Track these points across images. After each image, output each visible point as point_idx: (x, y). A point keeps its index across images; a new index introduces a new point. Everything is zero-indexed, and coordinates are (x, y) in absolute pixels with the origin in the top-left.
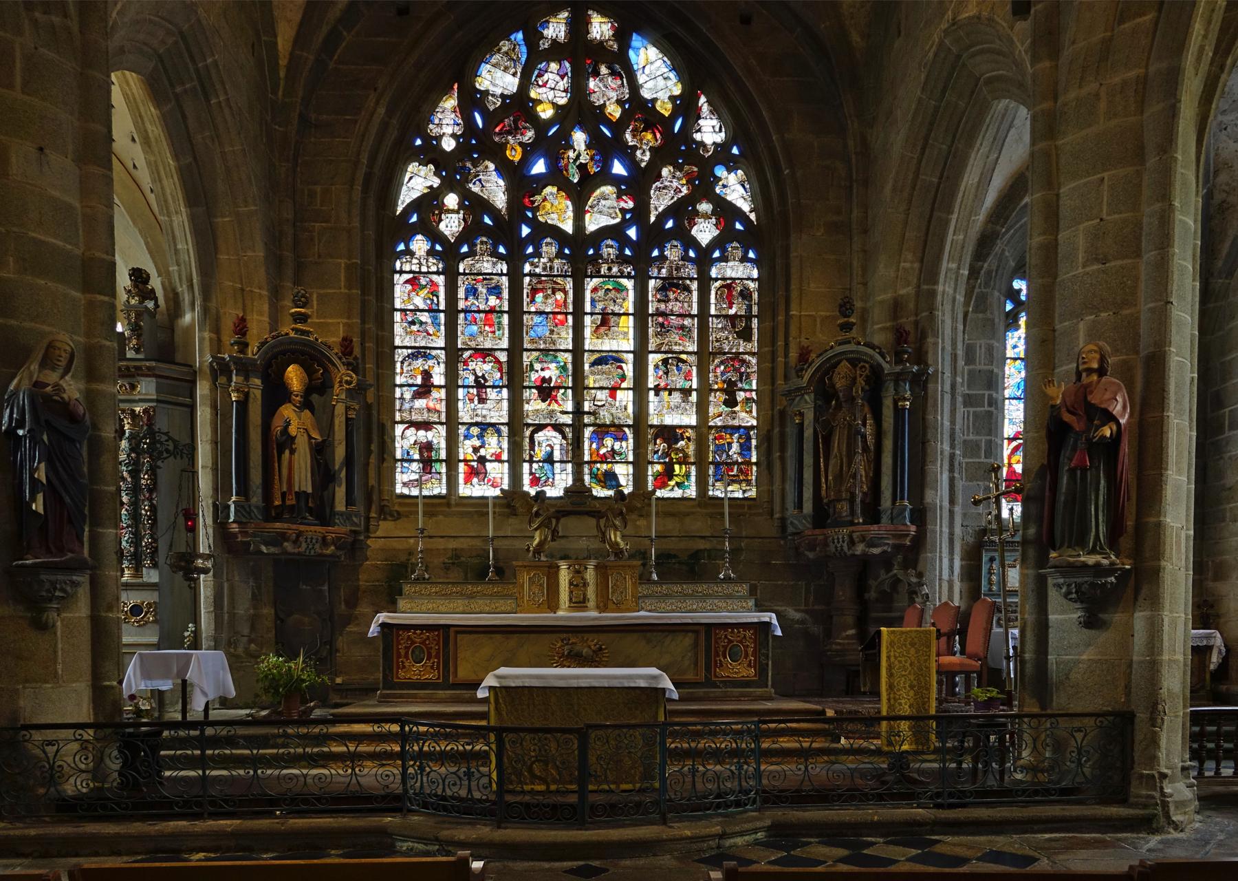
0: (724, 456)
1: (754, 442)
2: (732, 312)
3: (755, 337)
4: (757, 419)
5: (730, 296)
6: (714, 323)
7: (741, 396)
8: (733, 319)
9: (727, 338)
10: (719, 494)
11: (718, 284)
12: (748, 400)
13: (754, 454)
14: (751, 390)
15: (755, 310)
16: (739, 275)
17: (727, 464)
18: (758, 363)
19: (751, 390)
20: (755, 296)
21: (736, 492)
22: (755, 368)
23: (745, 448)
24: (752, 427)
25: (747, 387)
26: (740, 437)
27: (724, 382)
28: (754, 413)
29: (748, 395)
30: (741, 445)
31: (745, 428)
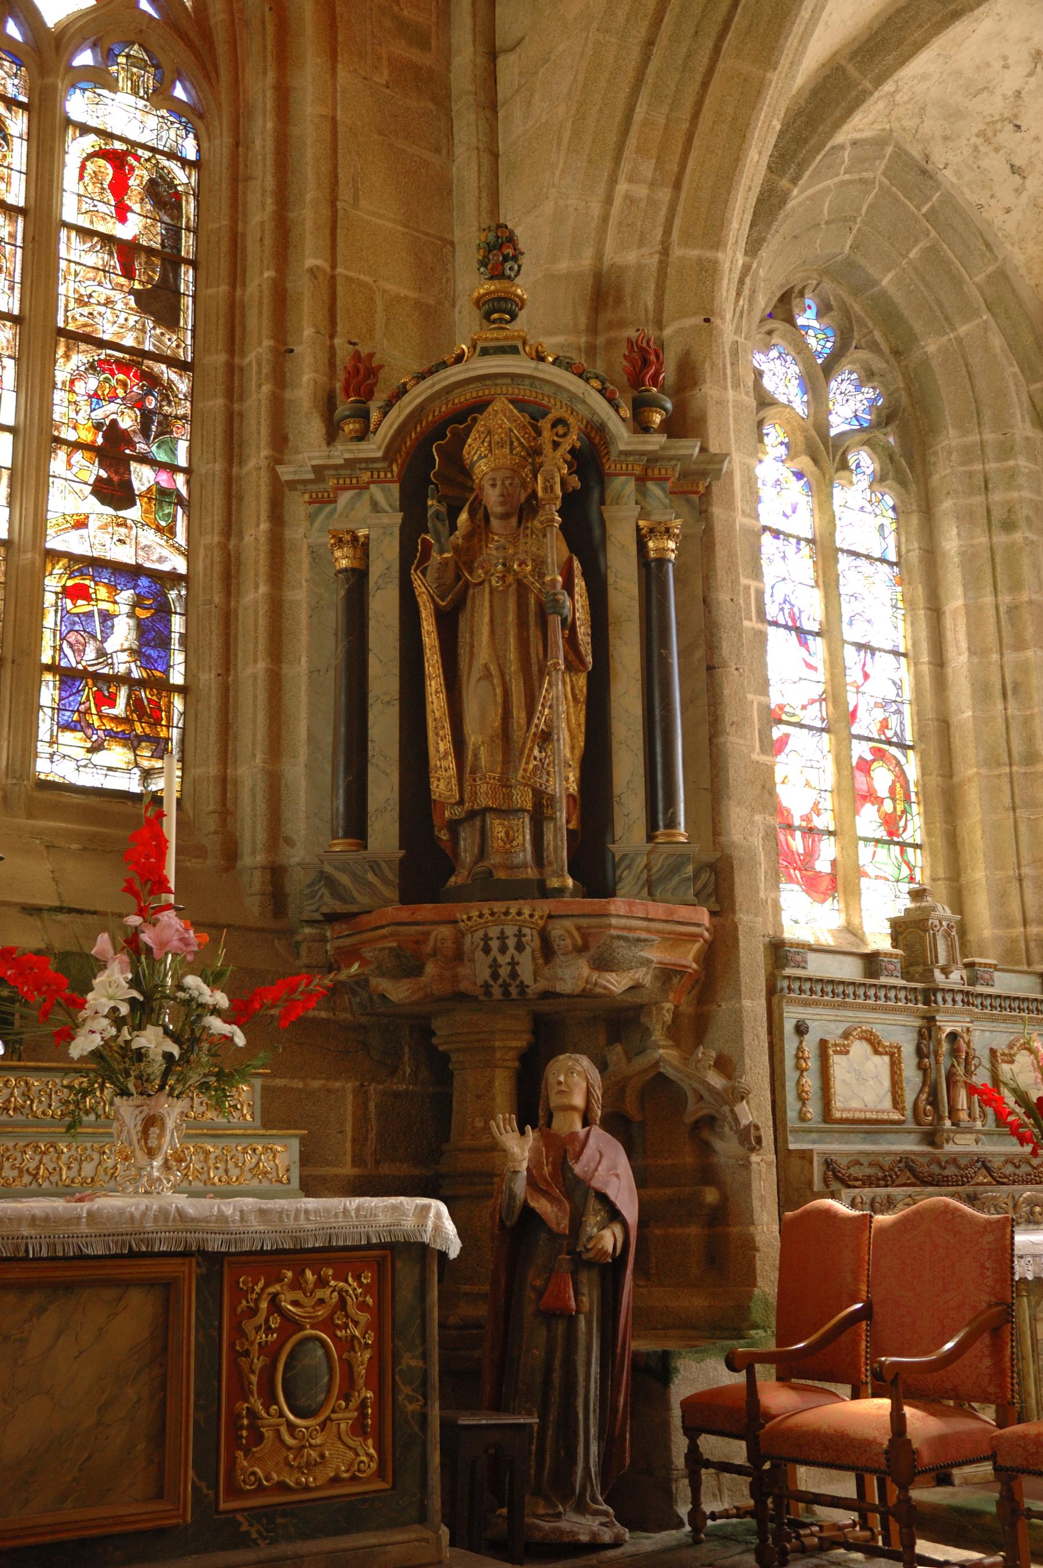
0: (90, 654)
1: (177, 624)
2: (126, 232)
3: (187, 319)
4: (188, 555)
5: (119, 187)
6: (71, 250)
7: (142, 477)
8: (127, 252)
9: (108, 302)
10: (64, 772)
11: (90, 143)
12: (162, 496)
13: (178, 658)
14: (174, 469)
15: (188, 244)
16: (145, 137)
17: (96, 676)
18: (192, 396)
19: (174, 469)
20: (189, 207)
21: (115, 770)
22: (184, 409)
23: (151, 638)
24: (174, 578)
25: (162, 457)
26: (137, 603)
27: (98, 426)
28: (181, 538)
29: (164, 479)
30: (142, 629)
31: (155, 575)
